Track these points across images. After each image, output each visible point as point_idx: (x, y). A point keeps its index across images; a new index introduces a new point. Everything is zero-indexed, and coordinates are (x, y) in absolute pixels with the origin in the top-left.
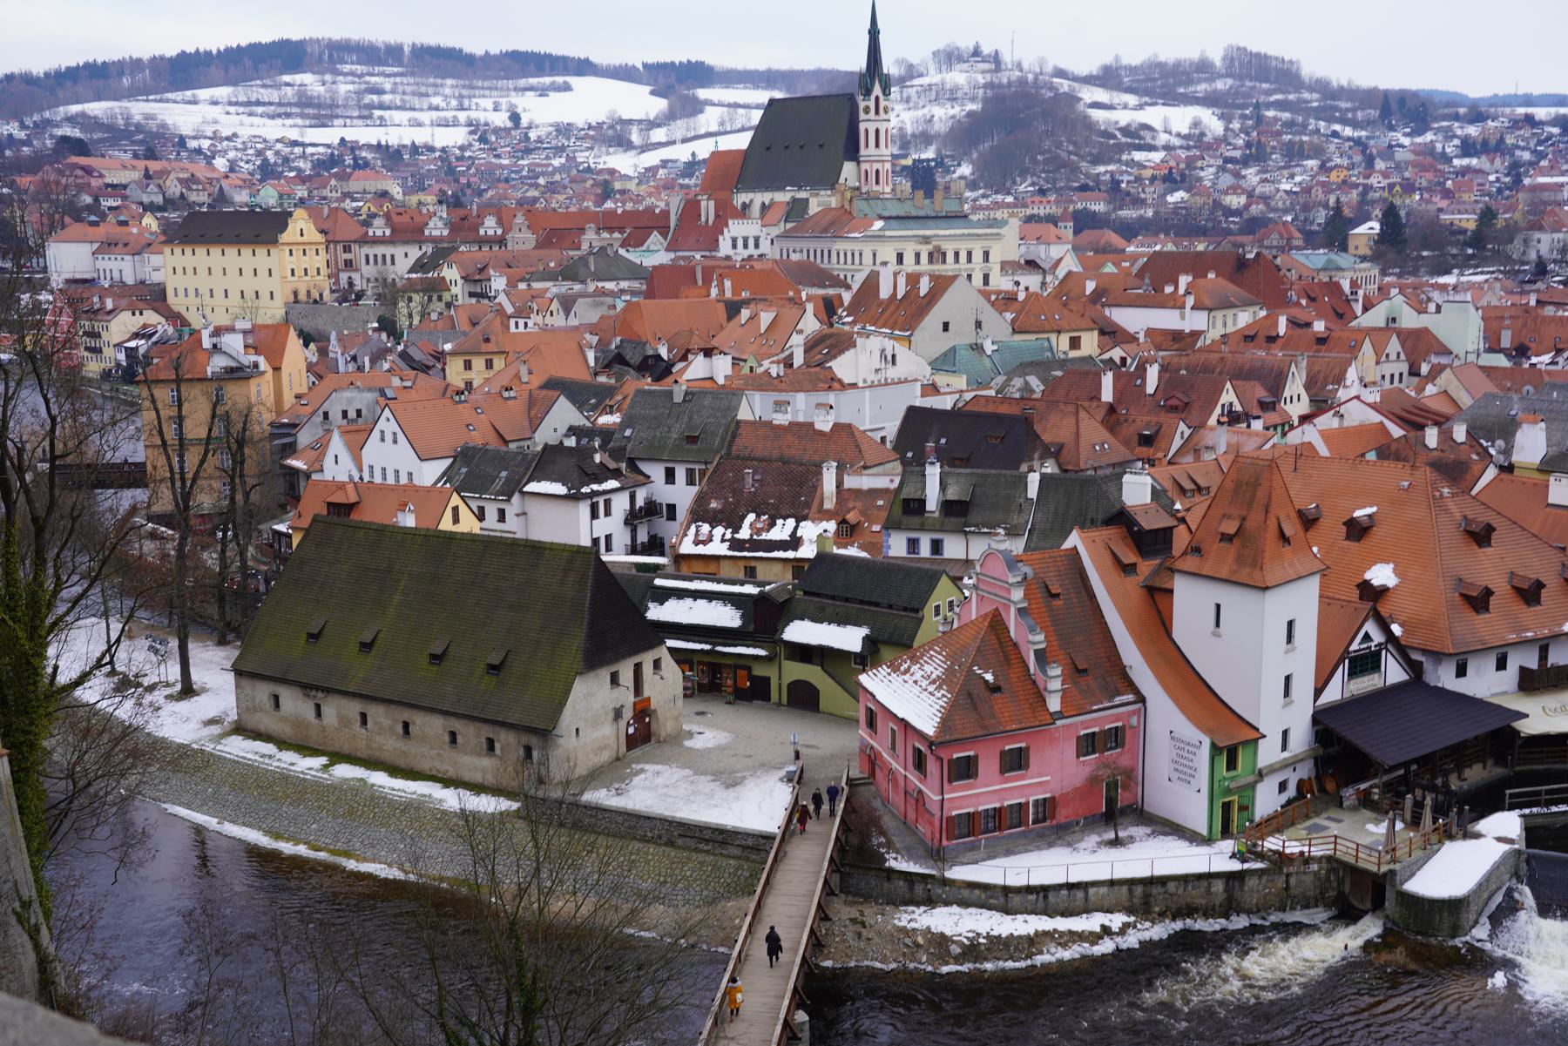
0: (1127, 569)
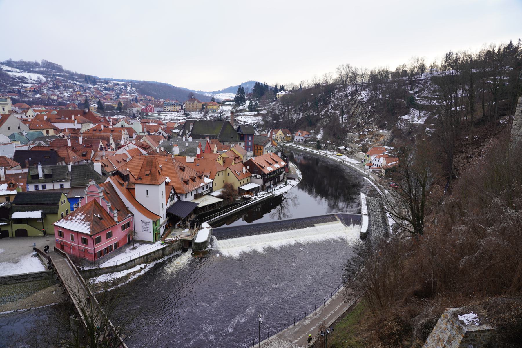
0: (122, 185)
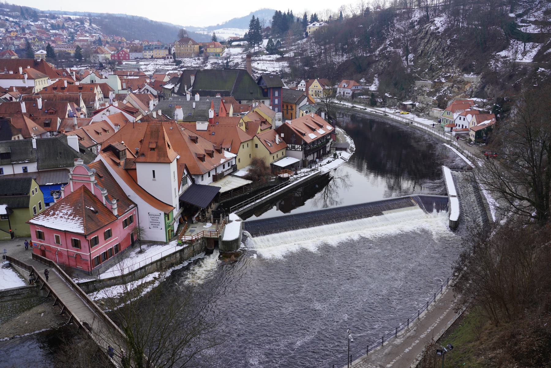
0: (118, 164)
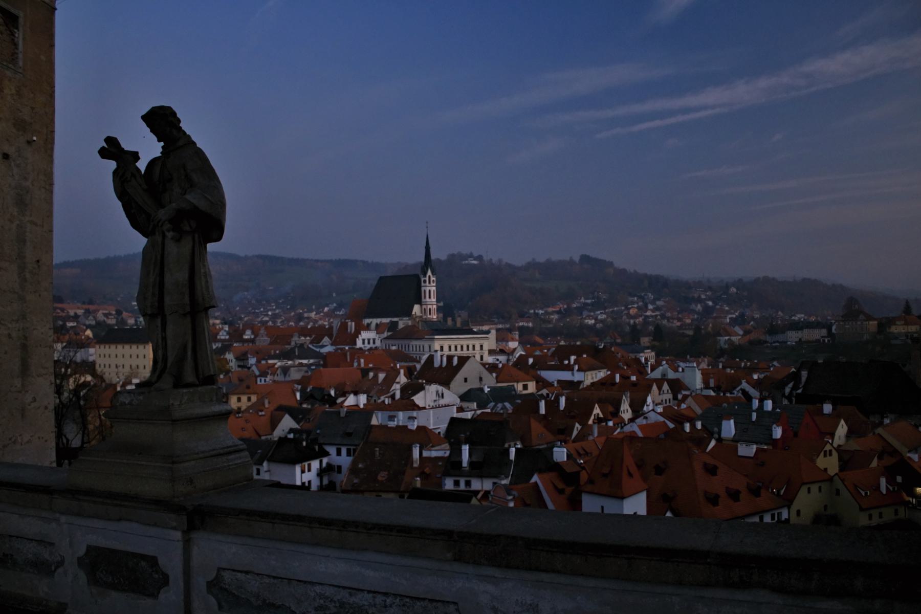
0: (561, 492)
